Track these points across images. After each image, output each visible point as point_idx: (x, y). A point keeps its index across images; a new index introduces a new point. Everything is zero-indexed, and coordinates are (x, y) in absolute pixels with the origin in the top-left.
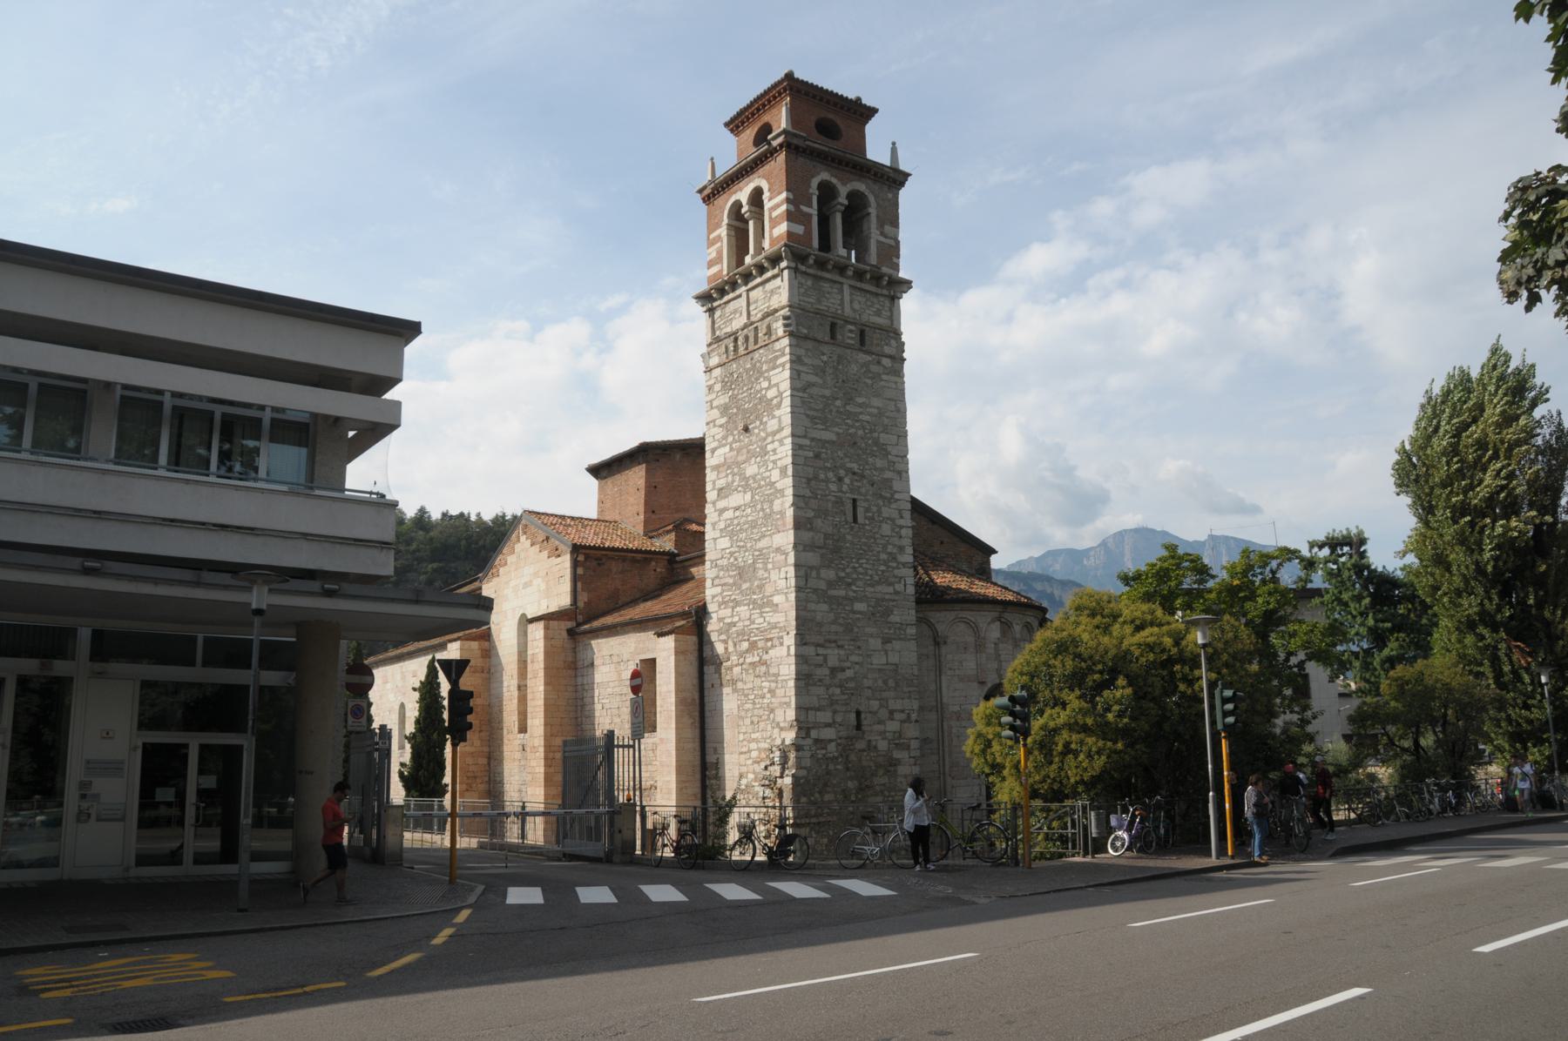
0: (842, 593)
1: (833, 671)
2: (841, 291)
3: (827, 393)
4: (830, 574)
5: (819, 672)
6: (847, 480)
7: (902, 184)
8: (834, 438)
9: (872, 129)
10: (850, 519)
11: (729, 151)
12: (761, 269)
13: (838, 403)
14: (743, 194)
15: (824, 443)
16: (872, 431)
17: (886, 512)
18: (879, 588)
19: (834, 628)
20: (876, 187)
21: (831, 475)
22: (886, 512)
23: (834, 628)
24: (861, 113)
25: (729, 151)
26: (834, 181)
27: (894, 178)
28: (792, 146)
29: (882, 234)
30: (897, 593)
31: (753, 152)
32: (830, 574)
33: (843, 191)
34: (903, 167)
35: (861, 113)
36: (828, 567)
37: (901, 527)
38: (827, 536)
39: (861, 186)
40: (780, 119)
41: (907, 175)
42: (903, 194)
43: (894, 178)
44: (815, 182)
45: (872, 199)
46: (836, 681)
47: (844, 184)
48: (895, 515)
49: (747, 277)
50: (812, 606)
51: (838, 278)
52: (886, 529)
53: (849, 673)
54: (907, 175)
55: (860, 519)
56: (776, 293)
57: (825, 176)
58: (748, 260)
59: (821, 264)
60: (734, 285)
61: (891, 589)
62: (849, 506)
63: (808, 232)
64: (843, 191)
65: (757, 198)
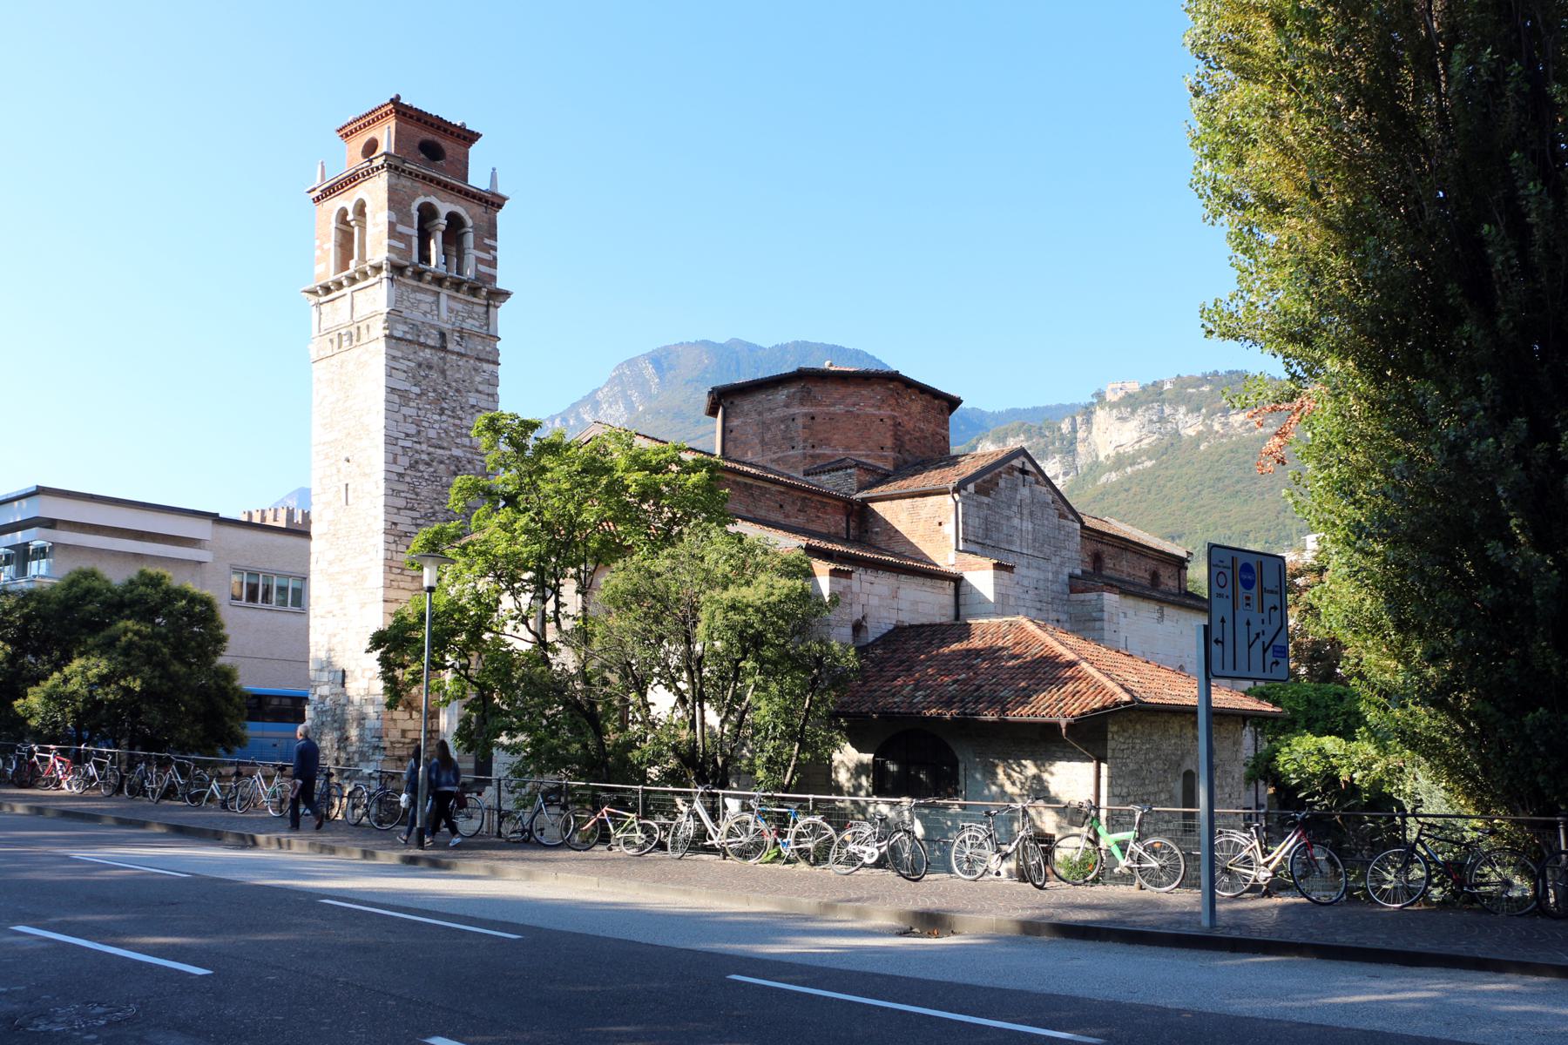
7: (500, 206)
9: (474, 151)
11: (349, 156)
12: (365, 275)
14: (347, 200)
24: (468, 137)
25: (349, 156)
27: (492, 202)
28: (394, 167)
31: (359, 162)
34: (501, 191)
35: (468, 137)
40: (385, 134)
41: (505, 199)
42: (501, 216)
43: (492, 202)
49: (353, 280)
51: (437, 289)
54: (505, 199)
56: (376, 298)
58: (352, 264)
59: (419, 275)
60: (340, 285)
63: (409, 246)
65: (361, 208)
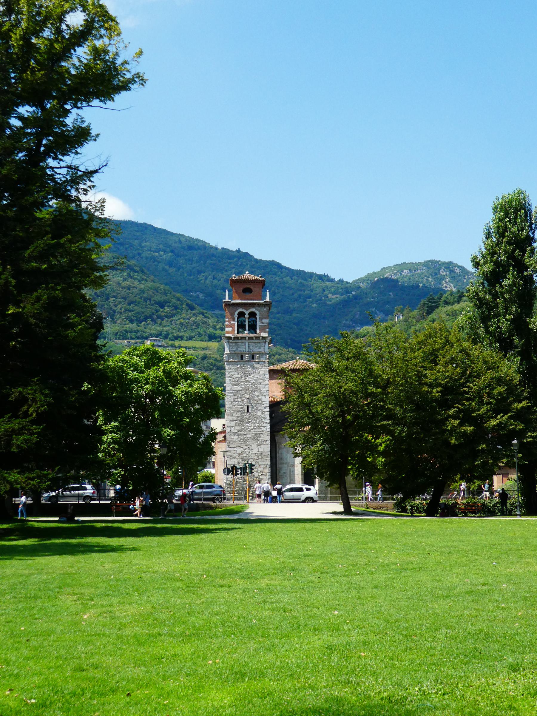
0: (243, 432)
1: (239, 454)
2: (245, 345)
3: (239, 376)
4: (239, 428)
5: (235, 455)
6: (245, 400)
8: (241, 389)
10: (246, 411)
13: (243, 379)
15: (237, 391)
16: (255, 385)
17: (259, 408)
18: (256, 430)
19: (240, 443)
20: (259, 308)
21: (240, 400)
22: (259, 408)
23: (240, 443)
26: (243, 310)
29: (262, 323)
30: (263, 431)
32: (239, 428)
33: (247, 313)
36: (238, 426)
37: (265, 412)
38: (238, 417)
39: (253, 310)
44: (236, 313)
45: (258, 313)
46: (240, 457)
47: (247, 310)
48: (263, 408)
50: (232, 437)
52: (259, 413)
53: (245, 455)
55: (250, 411)
57: (240, 310)
61: (261, 430)
62: (246, 408)
64: (247, 313)
